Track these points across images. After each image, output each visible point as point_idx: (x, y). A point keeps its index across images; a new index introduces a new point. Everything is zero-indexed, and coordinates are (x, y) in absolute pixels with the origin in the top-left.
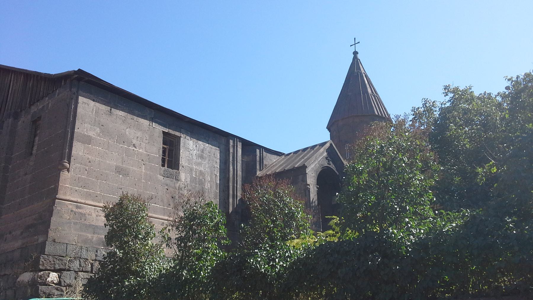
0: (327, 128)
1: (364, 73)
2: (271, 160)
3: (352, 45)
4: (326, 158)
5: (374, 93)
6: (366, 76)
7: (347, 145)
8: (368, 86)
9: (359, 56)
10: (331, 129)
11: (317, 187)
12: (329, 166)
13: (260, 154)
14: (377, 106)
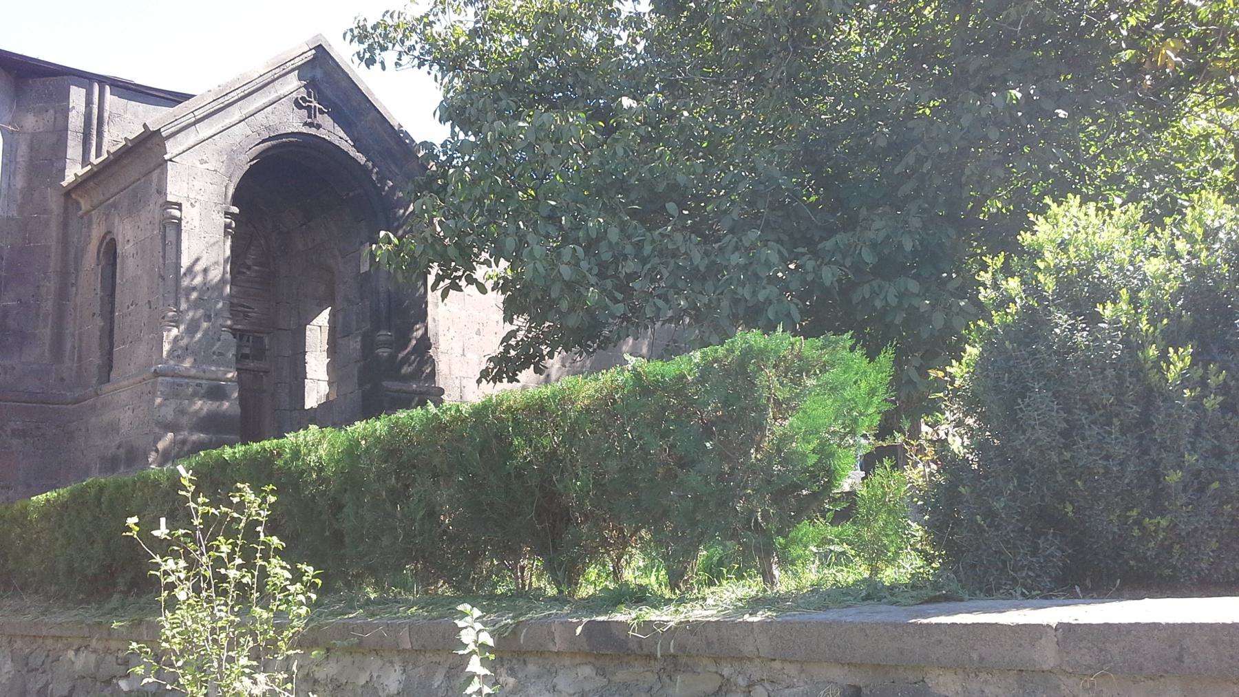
11: (226, 213)
12: (313, 131)
13: (89, 103)
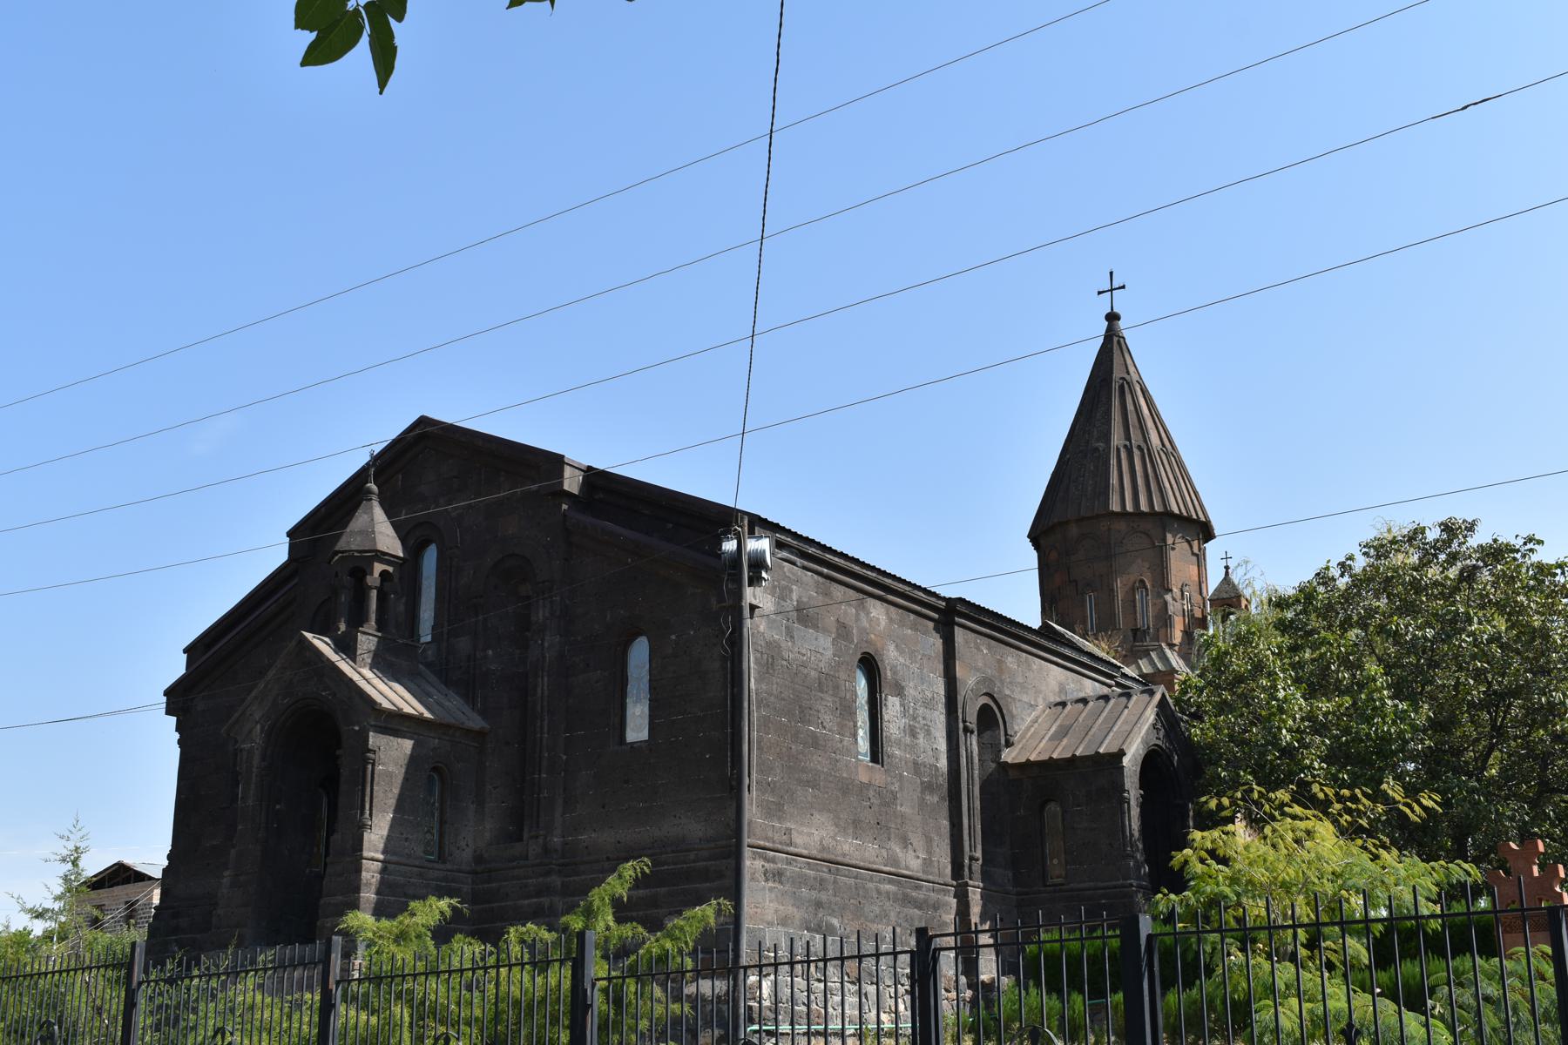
0: (1029, 536)
1: (1137, 381)
2: (1023, 719)
3: (1101, 290)
4: (1154, 726)
5: (1163, 445)
6: (1144, 391)
7: (1090, 596)
8: (1150, 423)
10: (1042, 542)
14: (1175, 486)
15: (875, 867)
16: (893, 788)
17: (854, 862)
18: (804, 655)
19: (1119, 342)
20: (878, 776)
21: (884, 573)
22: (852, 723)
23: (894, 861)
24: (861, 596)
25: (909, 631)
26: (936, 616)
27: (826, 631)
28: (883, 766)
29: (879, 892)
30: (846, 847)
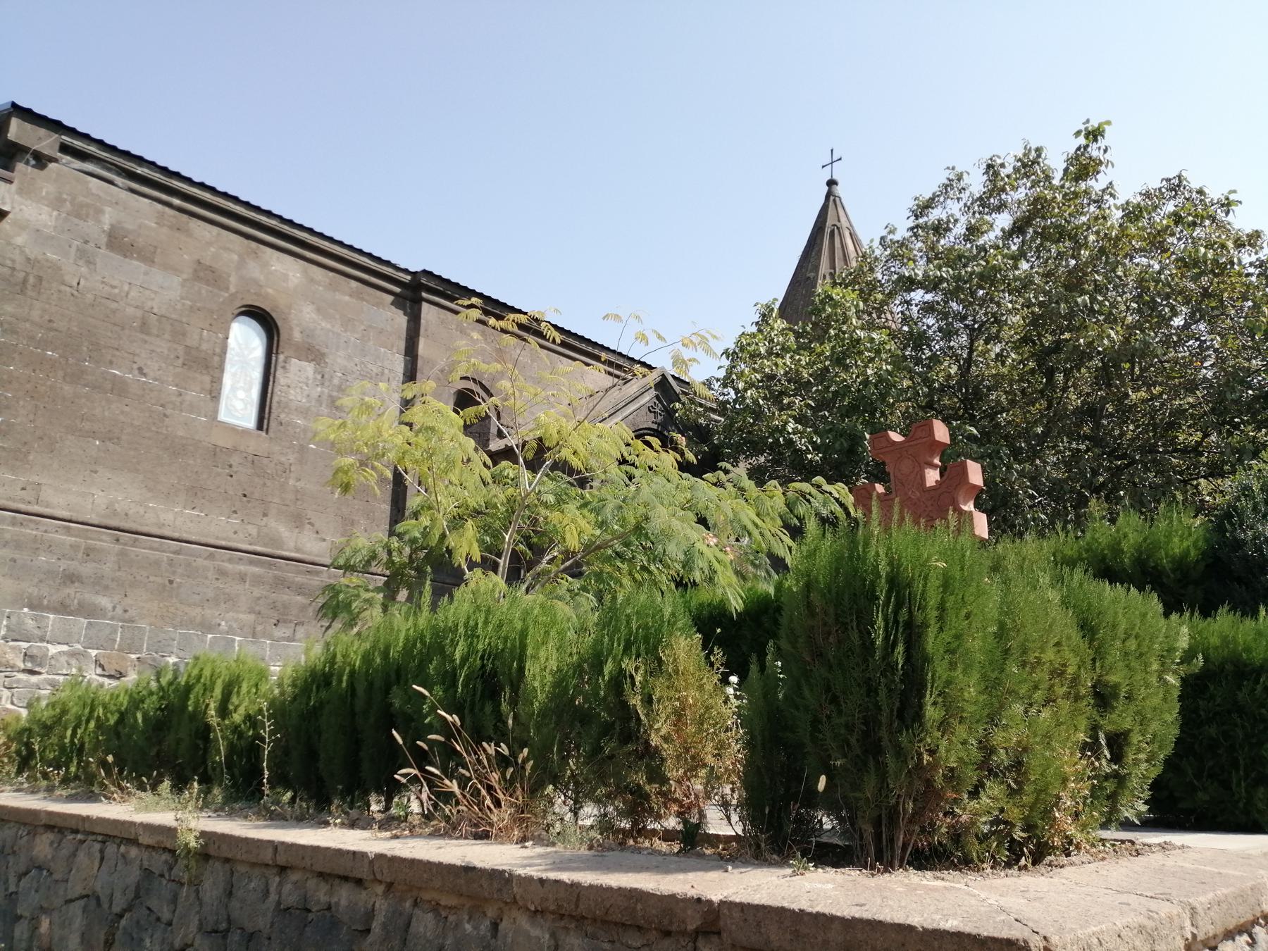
9: (839, 190)
15: (223, 543)
16: (283, 459)
17: (176, 535)
18: (113, 287)
19: (834, 200)
20: (261, 444)
21: (290, 223)
22: (207, 379)
23: (276, 541)
24: (254, 244)
25: (347, 298)
26: (397, 290)
27: (176, 271)
28: (267, 433)
29: (222, 573)
30: (168, 517)
